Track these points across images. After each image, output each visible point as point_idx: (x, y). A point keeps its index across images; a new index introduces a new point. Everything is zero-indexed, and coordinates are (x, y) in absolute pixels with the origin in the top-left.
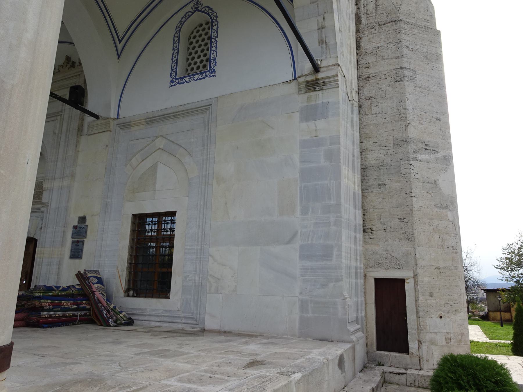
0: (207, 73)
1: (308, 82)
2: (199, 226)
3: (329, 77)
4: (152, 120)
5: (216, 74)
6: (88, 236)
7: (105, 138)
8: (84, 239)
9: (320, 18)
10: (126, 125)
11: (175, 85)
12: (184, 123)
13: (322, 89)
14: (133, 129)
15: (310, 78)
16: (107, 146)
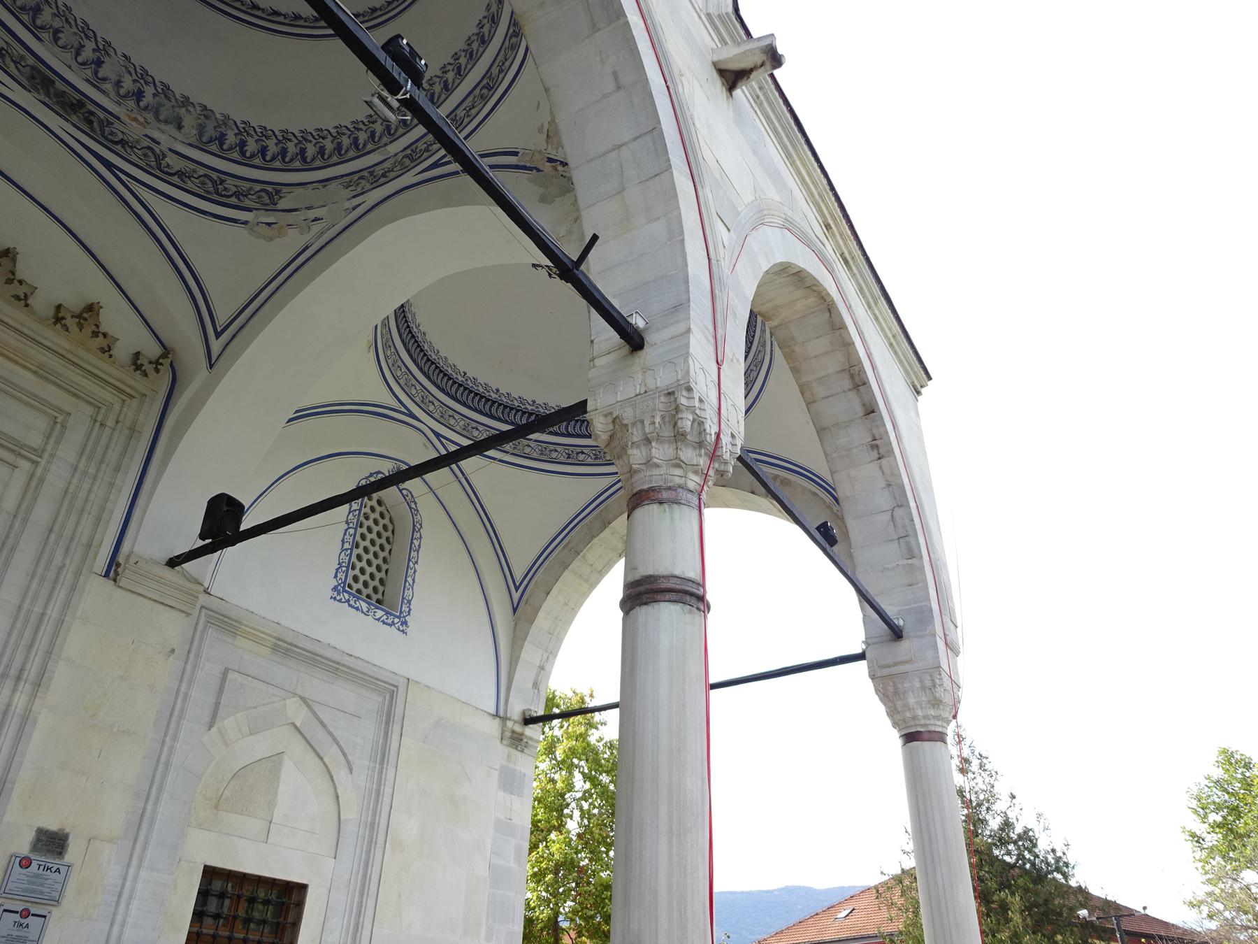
0: (396, 620)
1: (513, 732)
2: (348, 929)
3: (531, 739)
4: (288, 650)
5: (408, 631)
6: (65, 902)
7: (172, 626)
8: (54, 910)
9: (545, 655)
10: (226, 623)
11: (340, 601)
12: (346, 695)
13: (522, 751)
14: (240, 641)
15: (518, 728)
16: (173, 651)
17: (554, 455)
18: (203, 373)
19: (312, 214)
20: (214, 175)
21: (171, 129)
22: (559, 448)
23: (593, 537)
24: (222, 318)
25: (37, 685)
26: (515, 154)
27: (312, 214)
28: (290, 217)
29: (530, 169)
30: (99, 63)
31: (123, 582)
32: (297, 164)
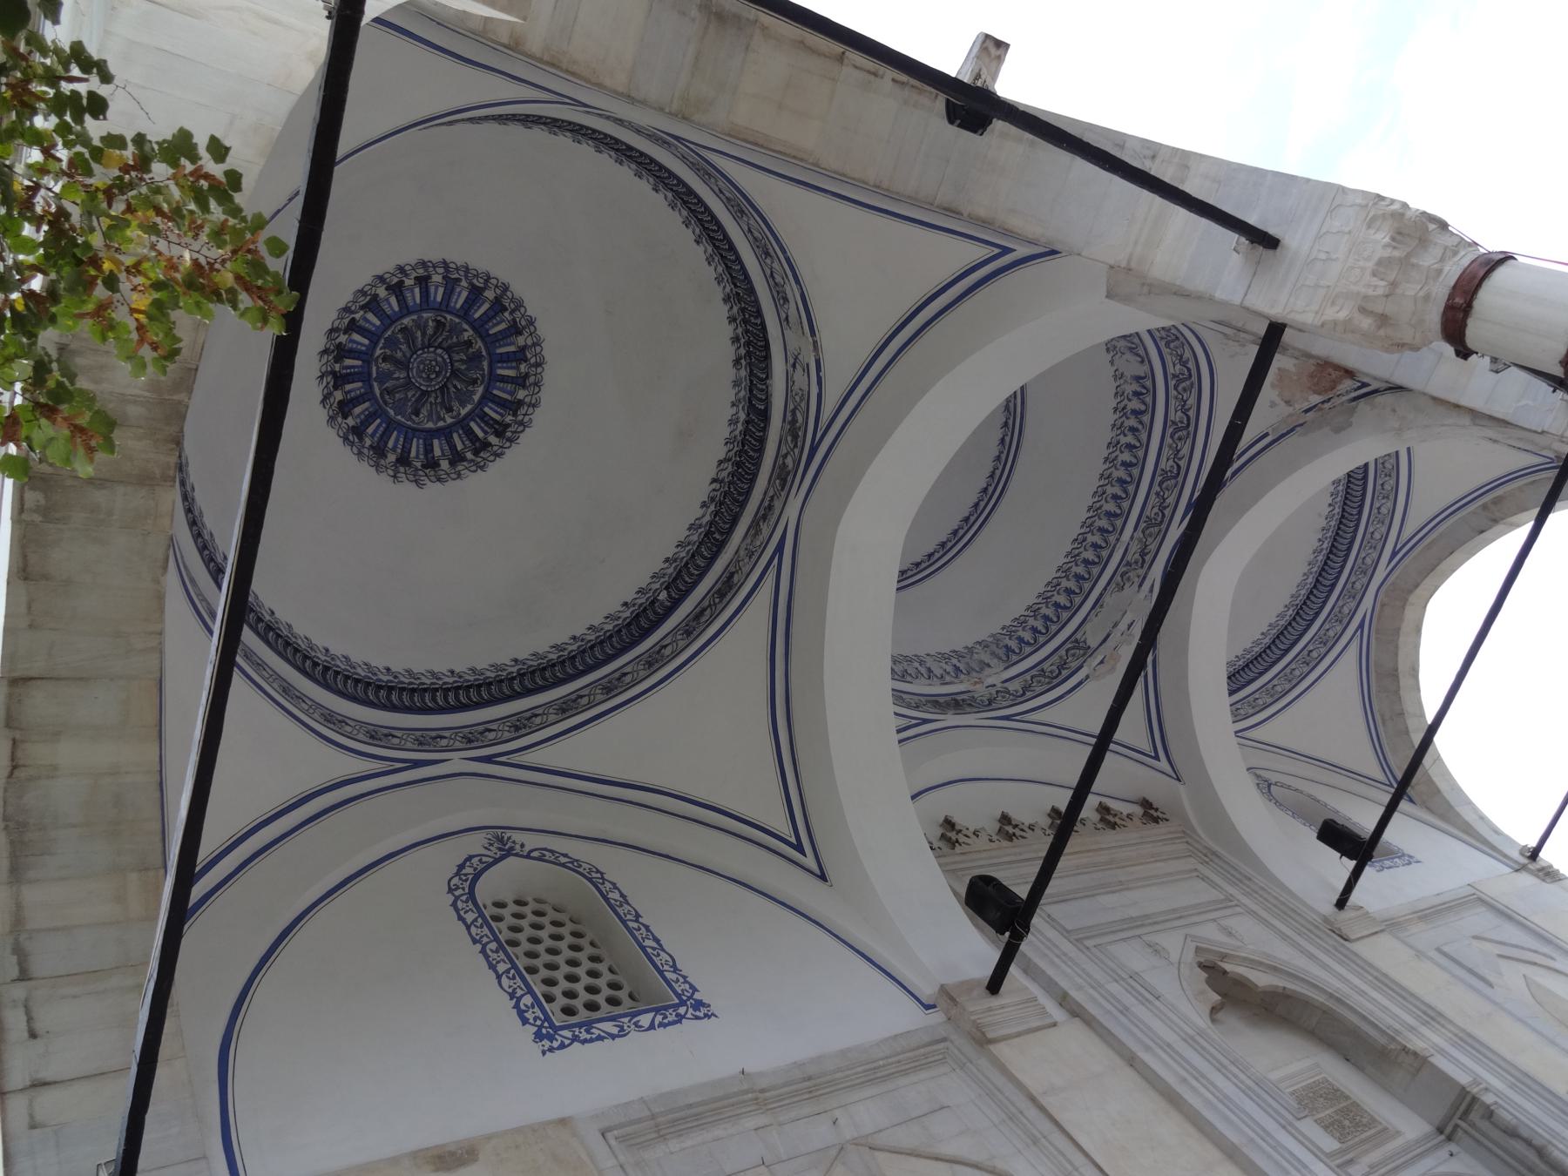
17: (1297, 673)
18: (1182, 790)
19: (1123, 626)
20: (1034, 672)
21: (987, 671)
22: (1293, 666)
23: (1397, 692)
24: (1147, 748)
25: (1440, 1014)
26: (1267, 435)
27: (1123, 626)
28: (1110, 643)
29: (1292, 430)
30: (930, 670)
31: (1352, 937)
32: (1065, 615)
